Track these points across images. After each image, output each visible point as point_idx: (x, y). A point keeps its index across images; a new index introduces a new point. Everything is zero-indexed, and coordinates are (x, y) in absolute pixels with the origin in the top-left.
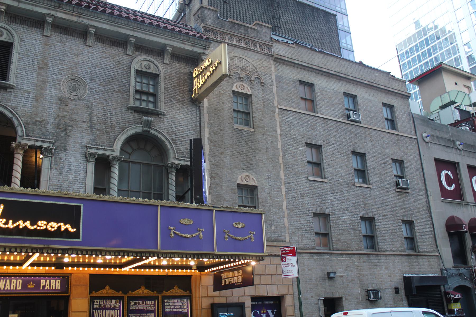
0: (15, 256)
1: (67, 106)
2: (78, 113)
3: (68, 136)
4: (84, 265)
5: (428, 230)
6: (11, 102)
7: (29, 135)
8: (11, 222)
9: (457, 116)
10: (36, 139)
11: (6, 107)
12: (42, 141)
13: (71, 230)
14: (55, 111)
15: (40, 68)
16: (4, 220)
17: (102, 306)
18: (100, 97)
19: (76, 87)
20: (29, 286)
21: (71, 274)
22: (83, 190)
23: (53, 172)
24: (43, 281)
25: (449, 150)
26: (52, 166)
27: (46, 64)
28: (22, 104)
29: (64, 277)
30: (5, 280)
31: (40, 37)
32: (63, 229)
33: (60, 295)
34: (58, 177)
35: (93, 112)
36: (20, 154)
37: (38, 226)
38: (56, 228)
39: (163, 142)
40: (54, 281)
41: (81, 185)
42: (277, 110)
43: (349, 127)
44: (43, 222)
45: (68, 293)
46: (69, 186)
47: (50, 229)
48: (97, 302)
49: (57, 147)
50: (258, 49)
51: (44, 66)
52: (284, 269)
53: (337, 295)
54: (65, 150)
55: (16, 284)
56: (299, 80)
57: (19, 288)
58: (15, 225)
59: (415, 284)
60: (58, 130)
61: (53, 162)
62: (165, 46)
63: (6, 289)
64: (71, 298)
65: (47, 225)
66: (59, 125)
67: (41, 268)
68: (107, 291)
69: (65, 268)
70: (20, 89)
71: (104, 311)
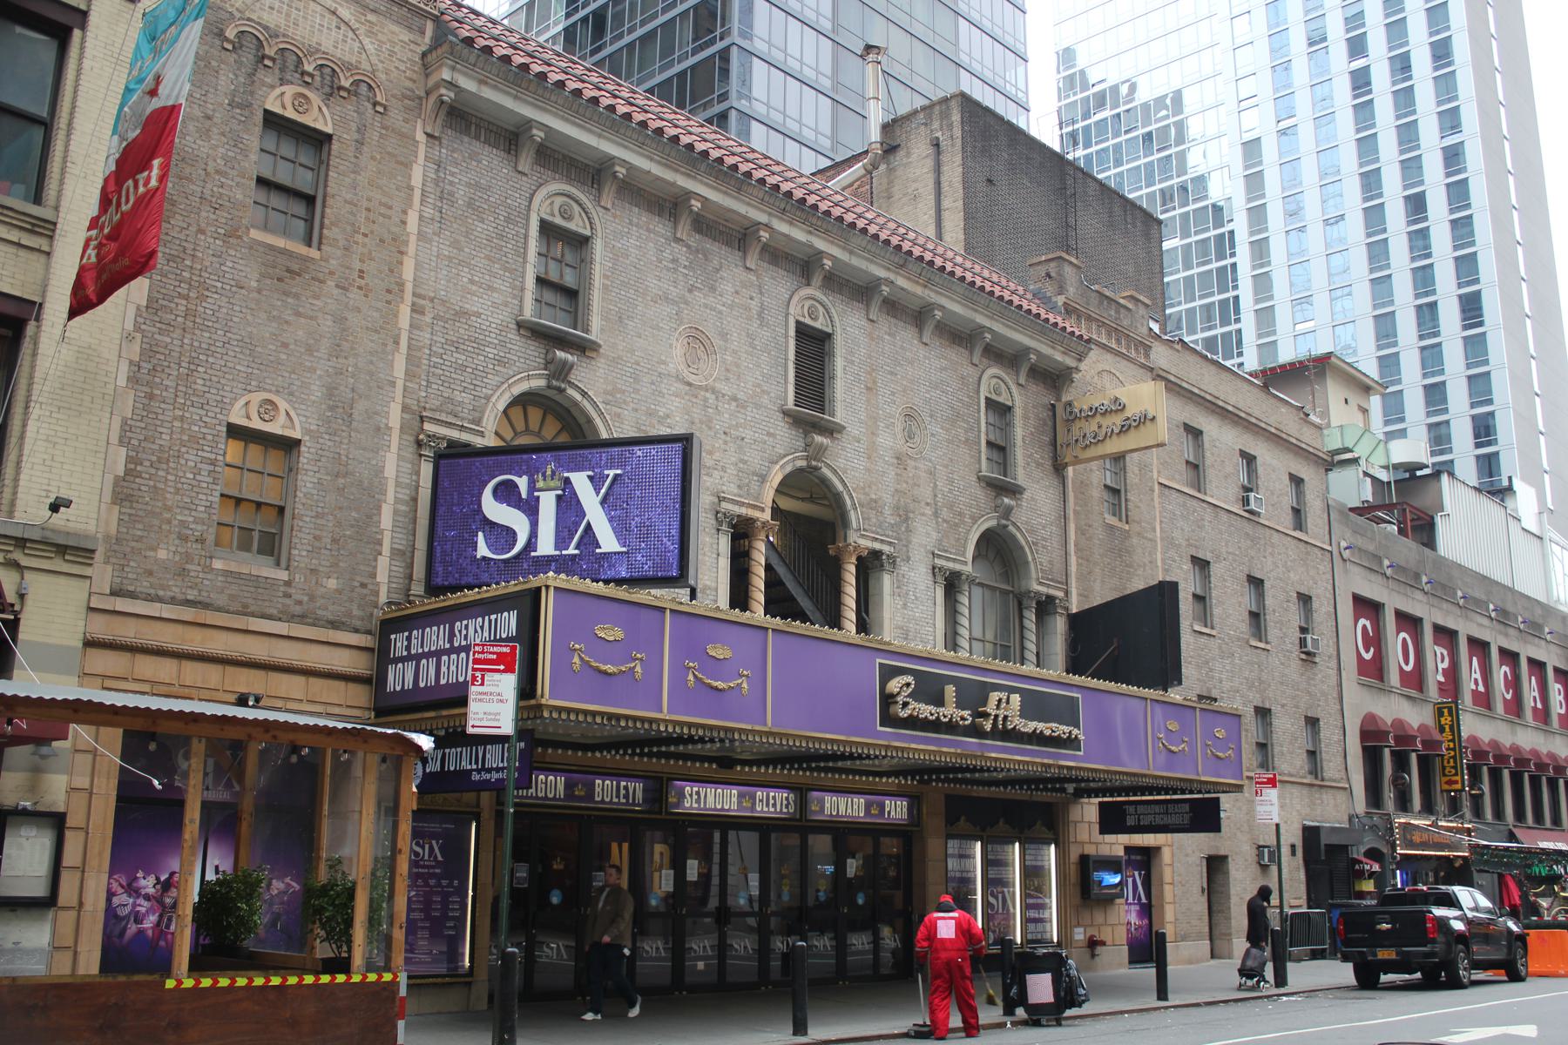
5: (1336, 738)
9: (1368, 494)
12: (882, 541)
15: (868, 389)
25: (1373, 577)
31: (864, 322)
39: (1022, 548)
42: (1156, 486)
43: (1245, 523)
50: (1133, 354)
52: (1259, 808)
53: (1222, 853)
54: (908, 559)
56: (1185, 424)
59: (1325, 840)
62: (1028, 350)
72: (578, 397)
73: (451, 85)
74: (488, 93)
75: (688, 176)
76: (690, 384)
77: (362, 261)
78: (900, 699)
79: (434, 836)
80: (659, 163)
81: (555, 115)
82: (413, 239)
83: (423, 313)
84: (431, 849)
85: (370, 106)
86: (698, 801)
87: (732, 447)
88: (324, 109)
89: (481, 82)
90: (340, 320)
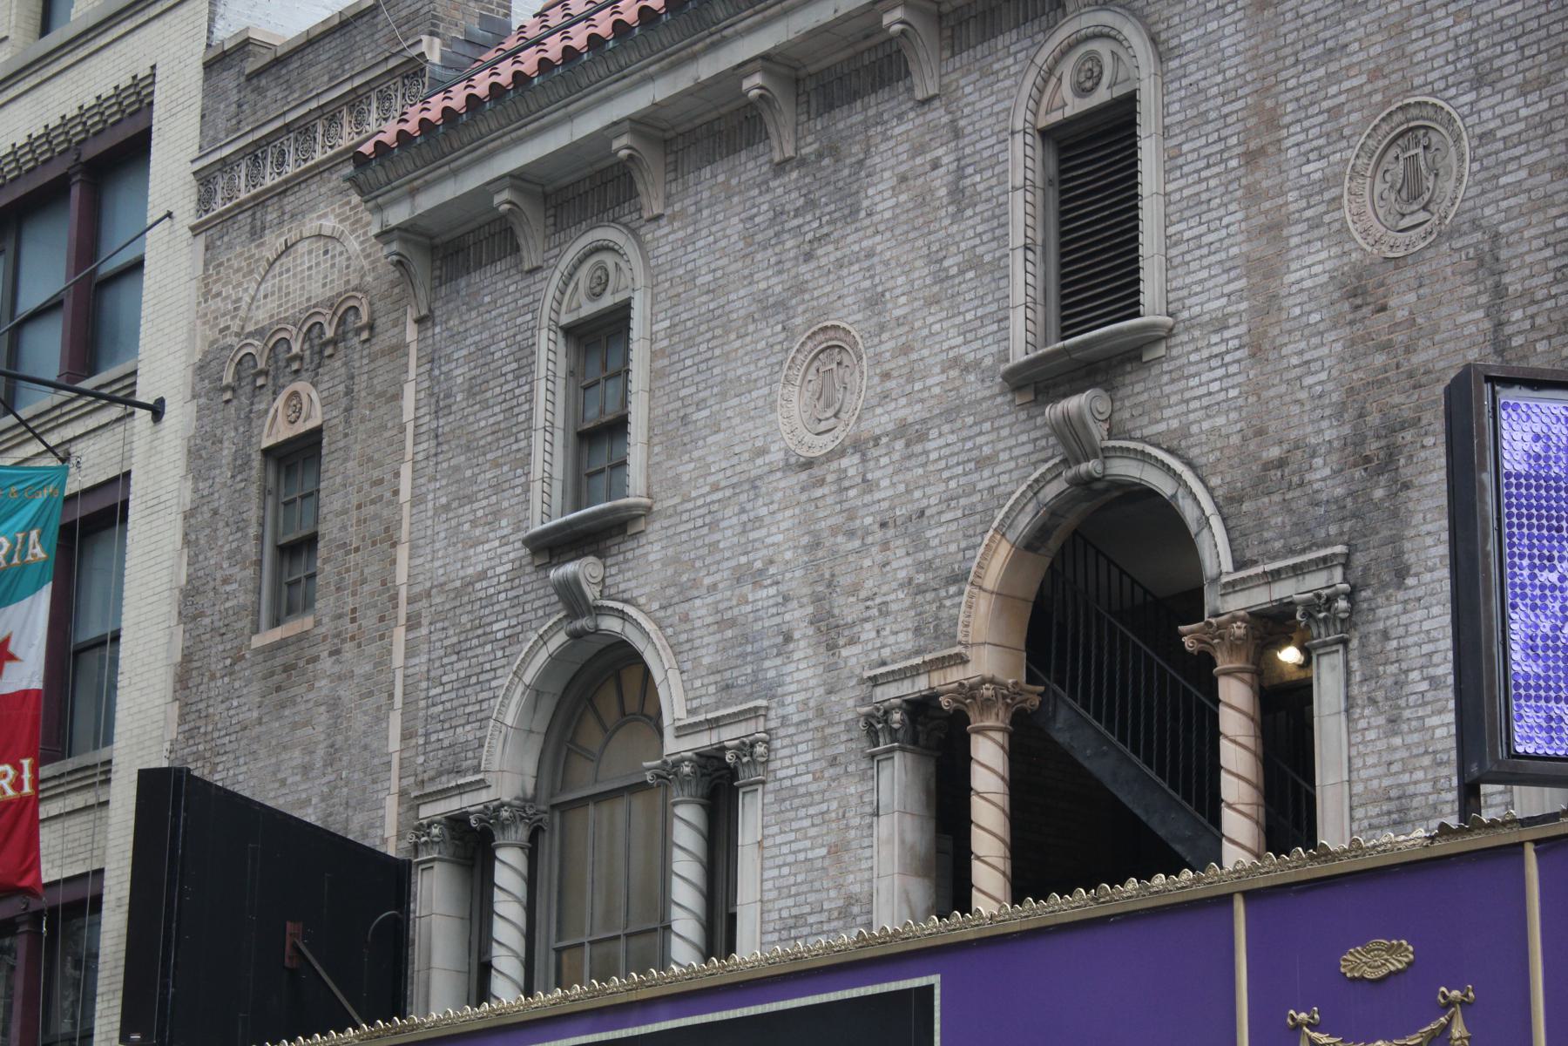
1: (1383, 308)
2: (1435, 330)
3: (1406, 486)
6: (1167, 413)
7: (1248, 554)
10: (1269, 567)
11: (1143, 452)
12: (1297, 571)
14: (1335, 373)
15: (1251, 158)
18: (1532, 170)
19: (1418, 170)
23: (1362, 724)
26: (1355, 690)
27: (1272, 122)
28: (1205, 402)
34: (1382, 745)
35: (1507, 279)
36: (1228, 673)
46: (1435, 781)
49: (1366, 569)
51: (1267, 139)
54: (1402, 573)
60: (1358, 473)
61: (1355, 665)
66: (1359, 440)
70: (1190, 325)
72: (611, 624)
73: (385, 235)
74: (427, 201)
75: (714, 46)
76: (809, 464)
77: (354, 594)
80: (664, 72)
81: (506, 148)
82: (407, 507)
83: (419, 625)
85: (355, 341)
87: (899, 547)
88: (314, 395)
89: (413, 193)
90: (334, 704)
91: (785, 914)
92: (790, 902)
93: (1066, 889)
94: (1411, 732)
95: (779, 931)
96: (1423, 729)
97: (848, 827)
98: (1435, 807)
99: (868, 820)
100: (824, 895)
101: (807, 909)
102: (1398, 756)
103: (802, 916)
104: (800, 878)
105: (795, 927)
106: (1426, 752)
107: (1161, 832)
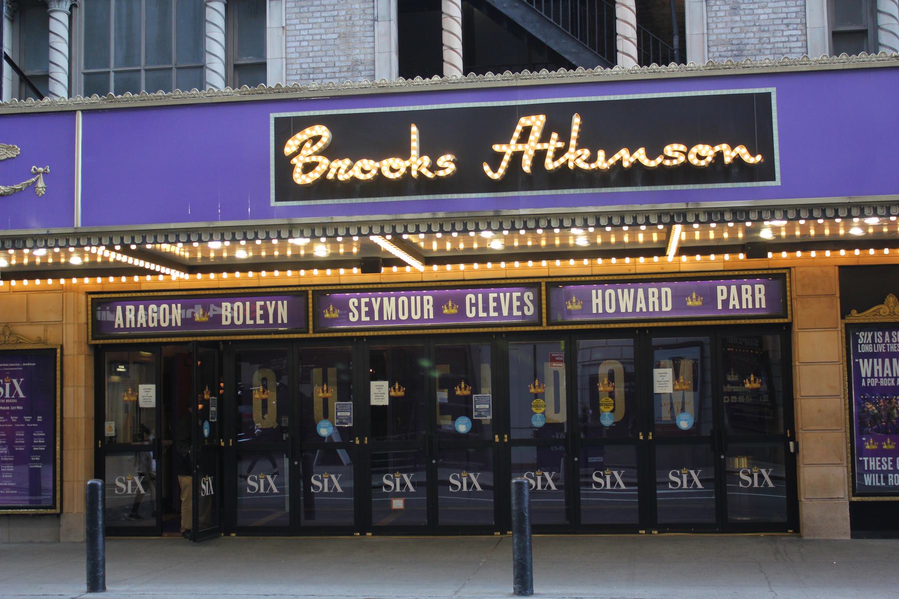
0: (455, 242)
4: (820, 244)
8: (601, 154)
13: (748, 158)
16: (586, 153)
17: (881, 348)
20: (690, 303)
21: (789, 268)
22: (799, 44)
24: (721, 288)
29: (775, 277)
30: (632, 290)
32: (727, 160)
33: (772, 321)
34: (728, 19)
37: (667, 158)
38: (709, 159)
40: (749, 287)
41: (794, 32)
44: (676, 146)
45: (786, 317)
46: (760, 39)
47: (695, 162)
48: (864, 337)
55: (660, 298)
57: (667, 308)
58: (612, 161)
63: (638, 310)
64: (795, 329)
65: (686, 154)
67: (712, 257)
68: (890, 308)
69: (770, 255)
71: (887, 360)
78: (298, 162)
79: (14, 375)
84: (12, 387)
86: (370, 313)
91: (304, 66)
92: (310, 60)
93: (498, 70)
94: (746, 15)
95: (301, 75)
96: (753, 14)
97: (353, 25)
98: (760, 50)
99: (370, 23)
100: (336, 59)
101: (323, 65)
102: (737, 25)
103: (319, 68)
104: (316, 49)
105: (313, 73)
106: (755, 25)
107: (555, 48)
